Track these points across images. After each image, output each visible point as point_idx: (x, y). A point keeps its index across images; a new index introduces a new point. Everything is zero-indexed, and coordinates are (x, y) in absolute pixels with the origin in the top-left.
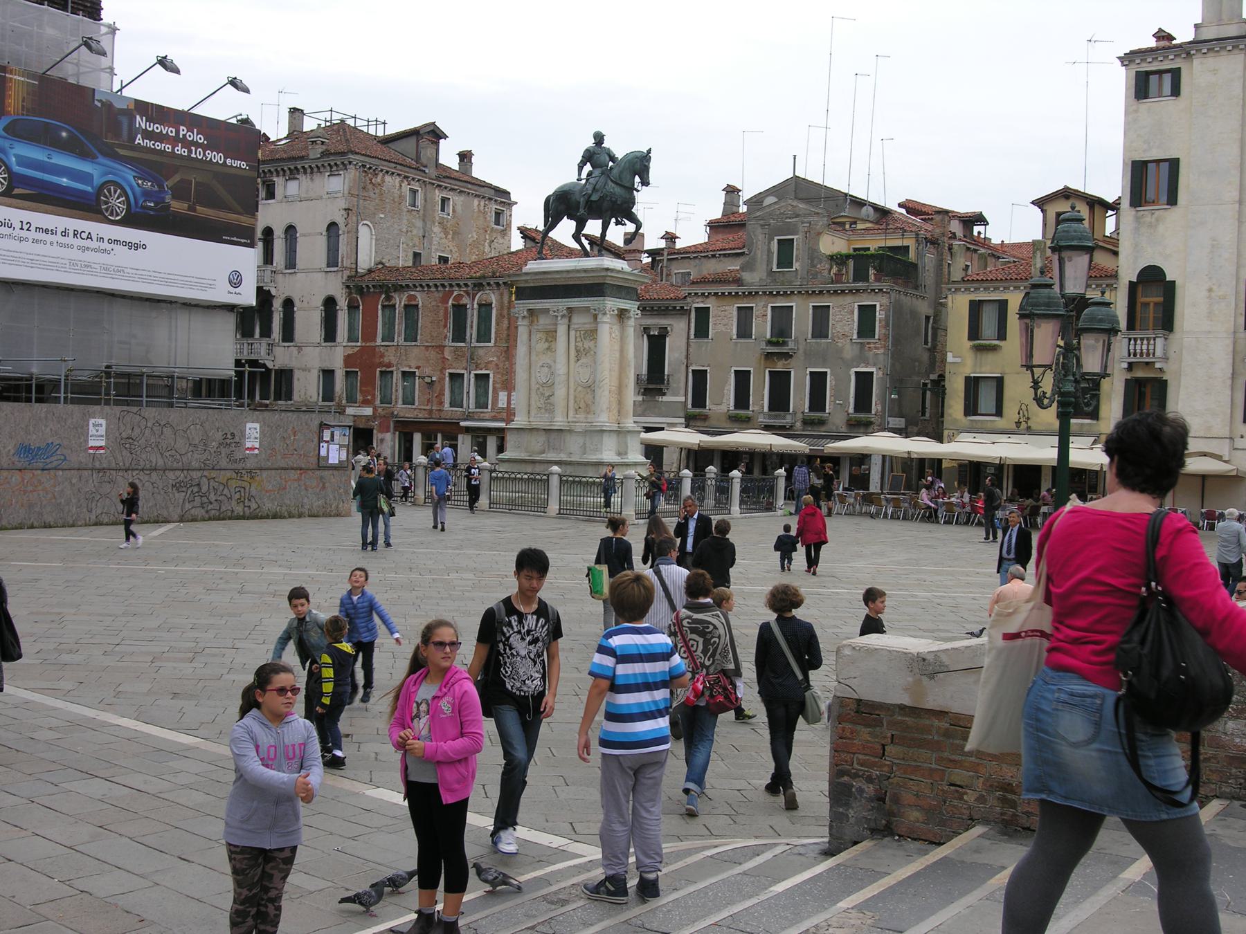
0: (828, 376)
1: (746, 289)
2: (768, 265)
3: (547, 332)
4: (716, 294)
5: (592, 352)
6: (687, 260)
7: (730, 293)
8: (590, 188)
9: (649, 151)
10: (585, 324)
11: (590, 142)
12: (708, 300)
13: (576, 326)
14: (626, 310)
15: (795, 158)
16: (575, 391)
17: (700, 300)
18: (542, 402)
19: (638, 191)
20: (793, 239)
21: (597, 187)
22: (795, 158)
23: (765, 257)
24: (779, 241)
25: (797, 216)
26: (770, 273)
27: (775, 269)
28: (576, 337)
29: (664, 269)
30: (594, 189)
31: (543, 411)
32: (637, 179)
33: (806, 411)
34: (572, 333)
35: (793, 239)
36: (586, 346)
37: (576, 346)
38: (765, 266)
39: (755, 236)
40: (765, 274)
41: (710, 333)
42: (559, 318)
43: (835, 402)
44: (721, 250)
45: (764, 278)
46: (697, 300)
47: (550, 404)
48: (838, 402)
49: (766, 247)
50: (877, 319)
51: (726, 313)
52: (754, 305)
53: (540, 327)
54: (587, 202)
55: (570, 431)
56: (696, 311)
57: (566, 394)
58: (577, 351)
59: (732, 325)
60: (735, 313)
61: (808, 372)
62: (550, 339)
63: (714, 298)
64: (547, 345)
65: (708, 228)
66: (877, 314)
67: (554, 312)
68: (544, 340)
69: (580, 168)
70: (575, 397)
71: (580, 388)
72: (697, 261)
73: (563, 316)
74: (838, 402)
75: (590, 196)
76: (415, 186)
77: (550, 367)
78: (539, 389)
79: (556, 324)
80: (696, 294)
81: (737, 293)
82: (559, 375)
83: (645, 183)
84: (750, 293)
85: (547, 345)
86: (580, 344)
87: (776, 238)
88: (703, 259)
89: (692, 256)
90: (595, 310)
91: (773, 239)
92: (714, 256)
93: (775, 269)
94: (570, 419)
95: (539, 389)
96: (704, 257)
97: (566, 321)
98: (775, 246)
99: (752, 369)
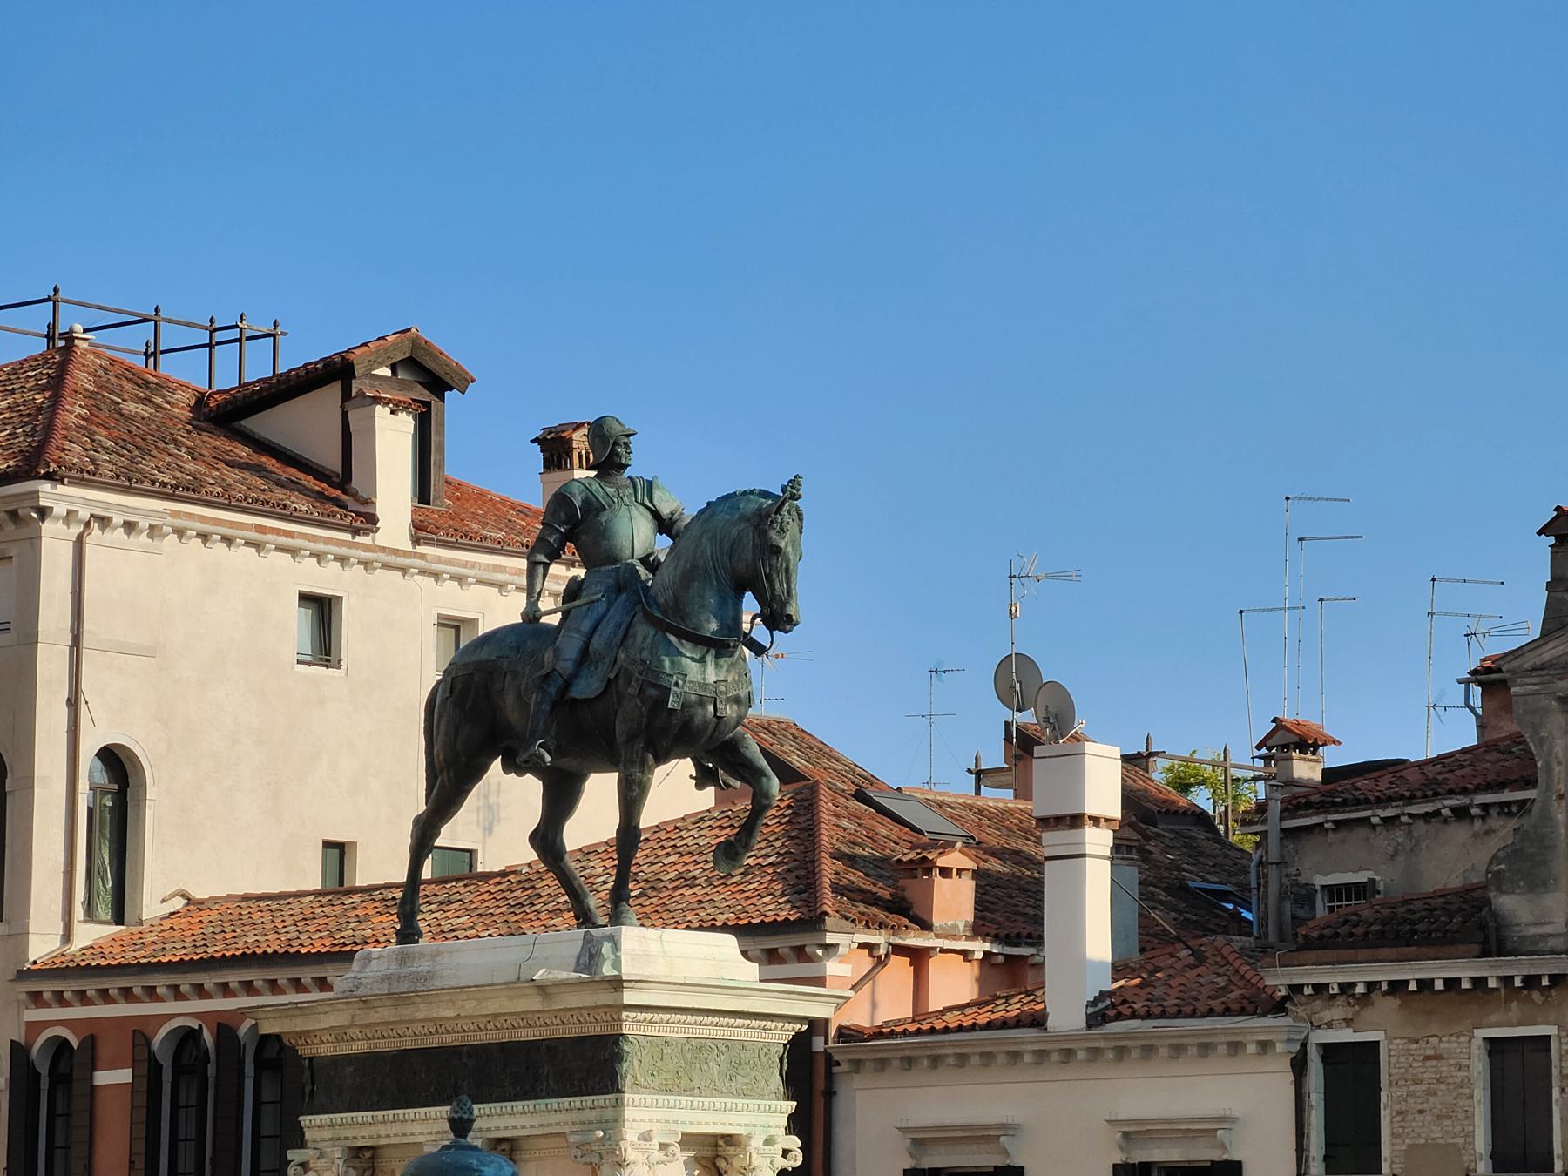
1: (1518, 969)
4: (1397, 987)
6: (1362, 832)
7: (1451, 984)
8: (570, 647)
9: (792, 490)
12: (1368, 1014)
14: (730, 1140)
17: (1337, 1012)
19: (759, 649)
21: (597, 643)
29: (1273, 872)
30: (585, 653)
32: (750, 605)
39: (1541, 741)
41: (1385, 1151)
44: (1489, 787)
46: (1327, 1015)
51: (1444, 1067)
52: (1550, 1030)
54: (554, 705)
56: (1324, 1059)
59: (1470, 1117)
60: (1480, 1066)
63: (1392, 1003)
65: (1477, 691)
72: (1399, 835)
75: (568, 684)
76: (323, 580)
80: (1320, 989)
81: (1479, 982)
83: (777, 619)
84: (1531, 981)
88: (1420, 824)
89: (1377, 815)
92: (1461, 813)
96: (1426, 817)
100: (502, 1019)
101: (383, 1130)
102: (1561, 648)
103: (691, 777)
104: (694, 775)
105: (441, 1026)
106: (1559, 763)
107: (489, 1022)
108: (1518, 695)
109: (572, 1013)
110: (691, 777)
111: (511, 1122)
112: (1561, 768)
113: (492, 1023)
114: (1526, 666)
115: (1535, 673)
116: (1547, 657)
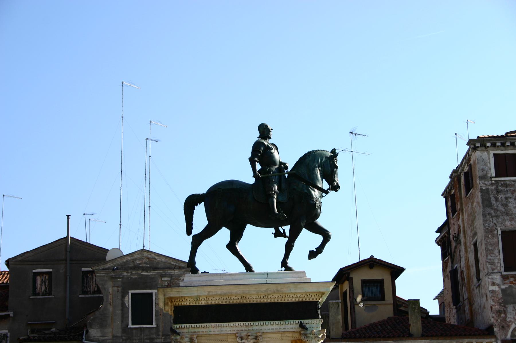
2: (122, 321)
11: (255, 135)
15: (68, 218)
20: (151, 294)
22: (68, 218)
23: (119, 312)
24: (132, 294)
25: (155, 269)
26: (125, 329)
27: (130, 326)
35: (151, 294)
38: (118, 322)
40: (120, 330)
45: (120, 335)
49: (120, 302)
83: (336, 188)
87: (131, 292)
91: (128, 293)
98: (128, 301)
100: (271, 295)
101: (212, 329)
102: (111, 265)
103: (273, 233)
104: (274, 233)
105: (244, 297)
106: (111, 295)
107: (266, 296)
108: (98, 276)
109: (302, 294)
110: (273, 233)
111: (272, 327)
112: (111, 296)
113: (267, 296)
114: (101, 269)
115: (104, 271)
116: (107, 267)
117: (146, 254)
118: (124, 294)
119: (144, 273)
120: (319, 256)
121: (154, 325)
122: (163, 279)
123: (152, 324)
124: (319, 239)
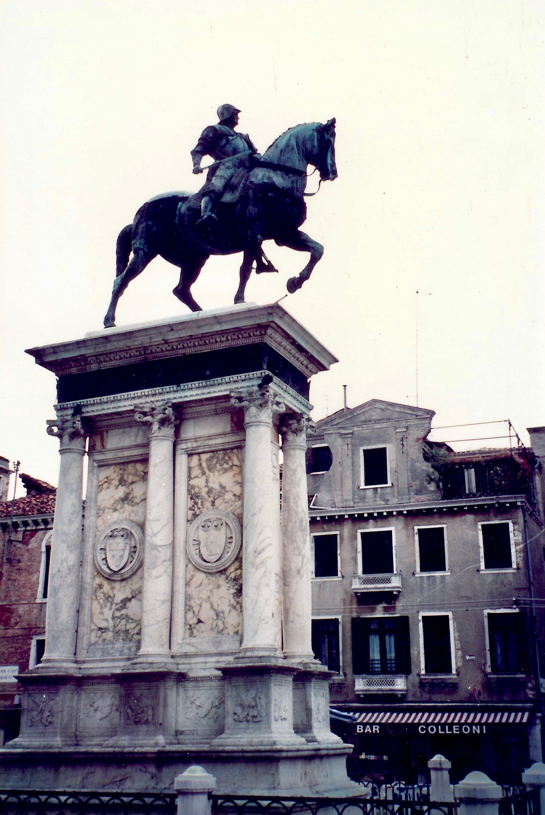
0: (451, 622)
3: (124, 464)
5: (229, 496)
10: (210, 437)
13: (189, 445)
15: (345, 389)
16: (187, 584)
18: (108, 613)
22: (345, 389)
28: (190, 469)
31: (109, 635)
33: (423, 672)
34: (182, 459)
36: (216, 486)
37: (190, 488)
42: (155, 426)
43: (463, 657)
47: (127, 618)
48: (468, 658)
50: (512, 542)
52: (337, 532)
53: (109, 456)
55: (181, 677)
57: (169, 590)
58: (193, 496)
61: (420, 618)
62: (130, 479)
64: (121, 492)
66: (511, 535)
67: (145, 414)
68: (116, 482)
69: (198, 153)
70: (188, 597)
71: (200, 577)
73: (163, 422)
74: (468, 658)
77: (128, 535)
78: (101, 586)
79: (147, 445)
82: (155, 547)
85: (121, 492)
86: (199, 482)
90: (240, 399)
91: (359, 450)
93: (363, 486)
94: (176, 649)
95: (101, 586)
97: (169, 431)
99: (340, 617)
117: (377, 405)
118: (354, 453)
119: (378, 426)
120: (306, 284)
121: (389, 484)
122: (397, 431)
123: (387, 483)
124: (306, 256)
